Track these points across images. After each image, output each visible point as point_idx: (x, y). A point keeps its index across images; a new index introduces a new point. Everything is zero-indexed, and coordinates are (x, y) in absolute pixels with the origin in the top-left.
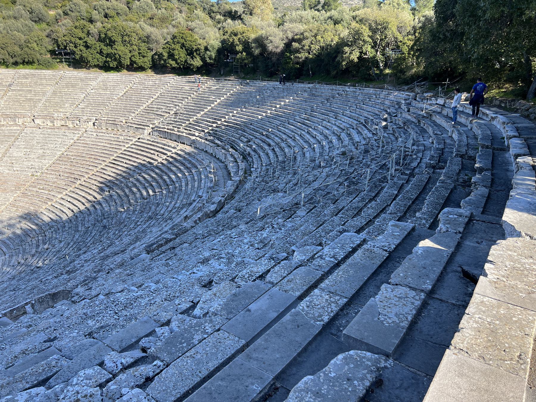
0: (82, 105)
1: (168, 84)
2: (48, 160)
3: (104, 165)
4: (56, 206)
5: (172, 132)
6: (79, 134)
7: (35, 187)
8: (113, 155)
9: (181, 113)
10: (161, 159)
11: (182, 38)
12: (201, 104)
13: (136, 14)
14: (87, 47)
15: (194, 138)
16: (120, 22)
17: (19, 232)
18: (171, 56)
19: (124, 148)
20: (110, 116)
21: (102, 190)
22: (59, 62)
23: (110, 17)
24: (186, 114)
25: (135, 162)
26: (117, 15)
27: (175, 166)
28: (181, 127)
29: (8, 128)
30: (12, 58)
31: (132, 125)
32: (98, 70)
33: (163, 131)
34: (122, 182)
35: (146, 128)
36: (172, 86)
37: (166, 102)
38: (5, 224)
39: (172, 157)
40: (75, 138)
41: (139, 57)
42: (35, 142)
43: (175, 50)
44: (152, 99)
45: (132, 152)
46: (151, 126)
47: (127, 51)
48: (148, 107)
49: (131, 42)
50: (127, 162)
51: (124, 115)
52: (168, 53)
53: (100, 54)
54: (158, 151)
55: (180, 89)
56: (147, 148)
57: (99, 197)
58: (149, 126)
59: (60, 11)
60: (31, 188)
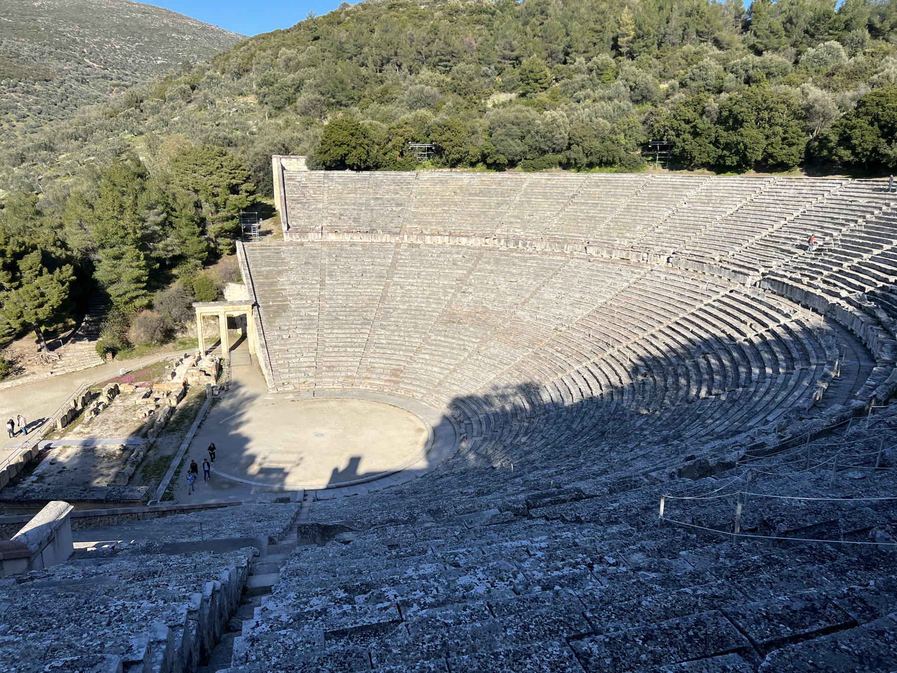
0: (661, 229)
1: (826, 194)
2: (584, 309)
3: (657, 329)
4: (566, 381)
5: (795, 284)
6: (639, 273)
7: (552, 347)
8: (676, 315)
9: (830, 250)
10: (752, 334)
11: (877, 104)
12: (880, 235)
13: (804, 71)
14: (695, 134)
15: (835, 300)
16: (772, 89)
17: (508, 408)
18: (845, 140)
19: (699, 305)
20: (697, 249)
21: (636, 370)
22: (652, 160)
23: (754, 82)
24: (841, 253)
25: (707, 331)
26: (767, 77)
27: (773, 353)
28: (819, 277)
29: (551, 258)
30: (587, 157)
31: (728, 266)
32: (706, 171)
33: (780, 282)
34: (670, 364)
35: (751, 272)
36: (833, 197)
37: (809, 227)
38: (500, 392)
39: (774, 333)
40: (632, 281)
41: (781, 146)
42: (575, 281)
43: (855, 128)
44: (783, 222)
45: (710, 314)
46: (762, 270)
47: (761, 137)
48: (771, 236)
49: (772, 121)
50: (696, 329)
51: (721, 248)
52: (841, 135)
53: (714, 145)
54: (754, 318)
55: (848, 203)
56: (738, 310)
57: (626, 381)
58: (757, 270)
59: (676, 82)
60: (546, 348)
